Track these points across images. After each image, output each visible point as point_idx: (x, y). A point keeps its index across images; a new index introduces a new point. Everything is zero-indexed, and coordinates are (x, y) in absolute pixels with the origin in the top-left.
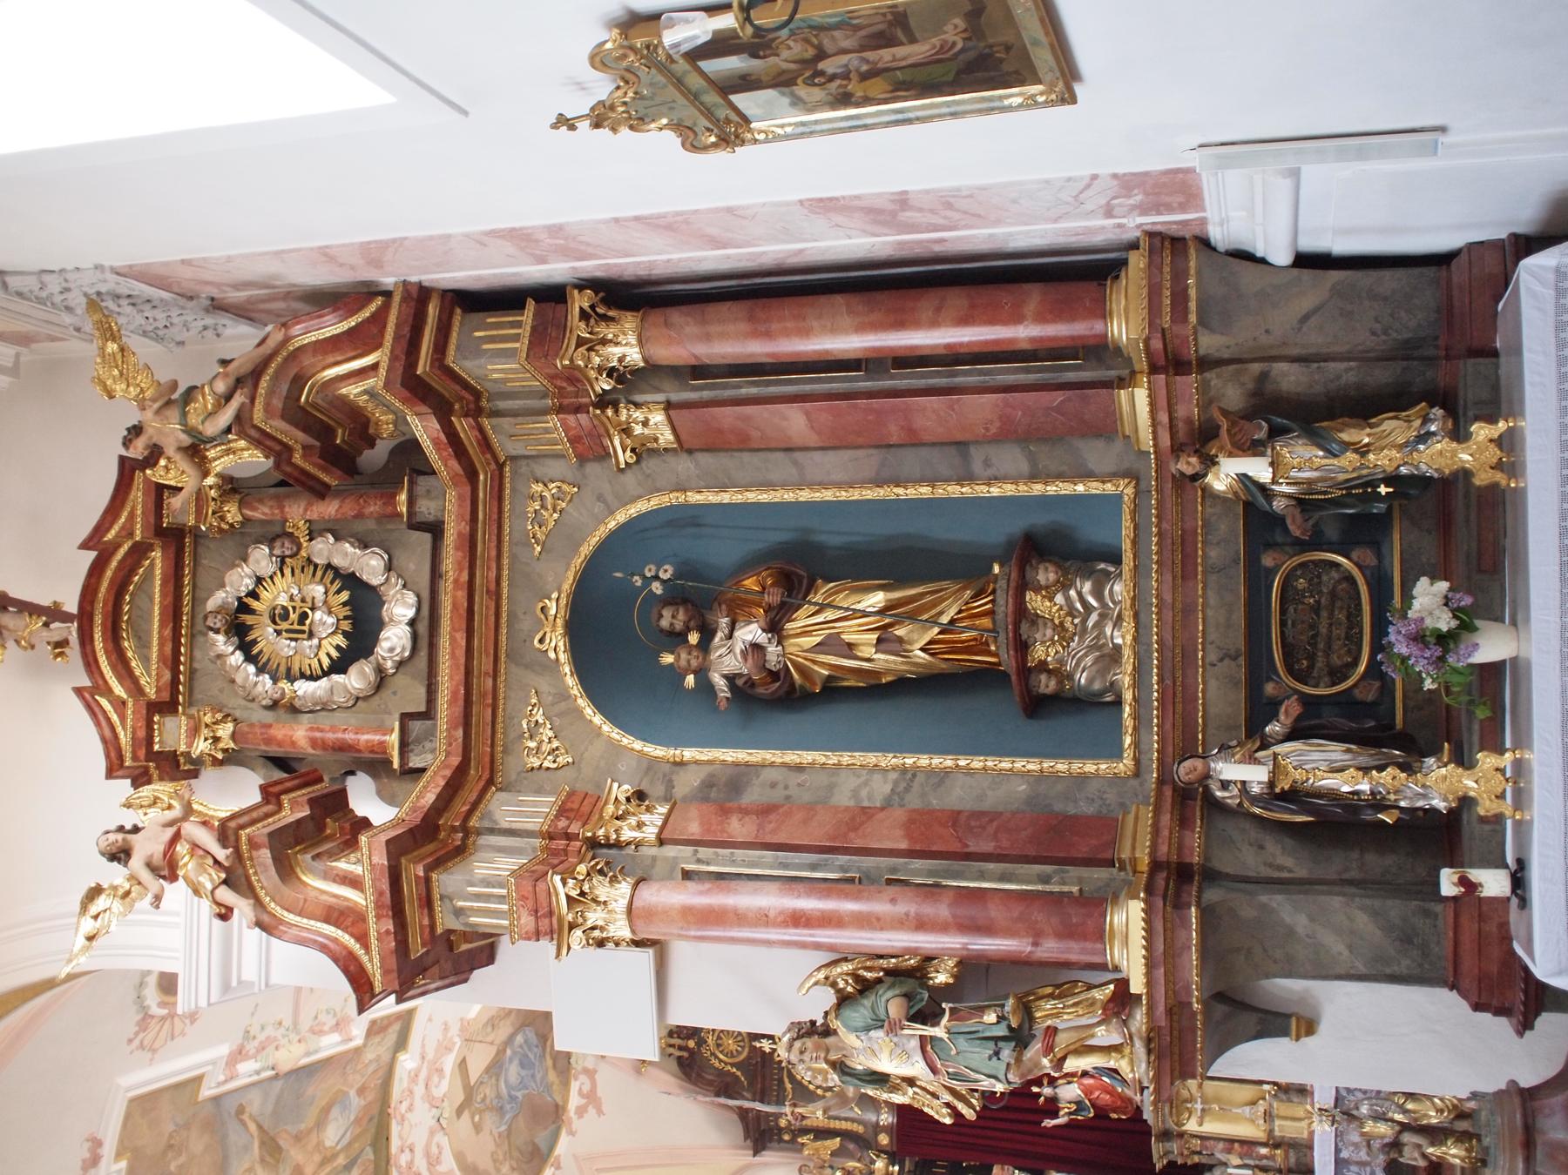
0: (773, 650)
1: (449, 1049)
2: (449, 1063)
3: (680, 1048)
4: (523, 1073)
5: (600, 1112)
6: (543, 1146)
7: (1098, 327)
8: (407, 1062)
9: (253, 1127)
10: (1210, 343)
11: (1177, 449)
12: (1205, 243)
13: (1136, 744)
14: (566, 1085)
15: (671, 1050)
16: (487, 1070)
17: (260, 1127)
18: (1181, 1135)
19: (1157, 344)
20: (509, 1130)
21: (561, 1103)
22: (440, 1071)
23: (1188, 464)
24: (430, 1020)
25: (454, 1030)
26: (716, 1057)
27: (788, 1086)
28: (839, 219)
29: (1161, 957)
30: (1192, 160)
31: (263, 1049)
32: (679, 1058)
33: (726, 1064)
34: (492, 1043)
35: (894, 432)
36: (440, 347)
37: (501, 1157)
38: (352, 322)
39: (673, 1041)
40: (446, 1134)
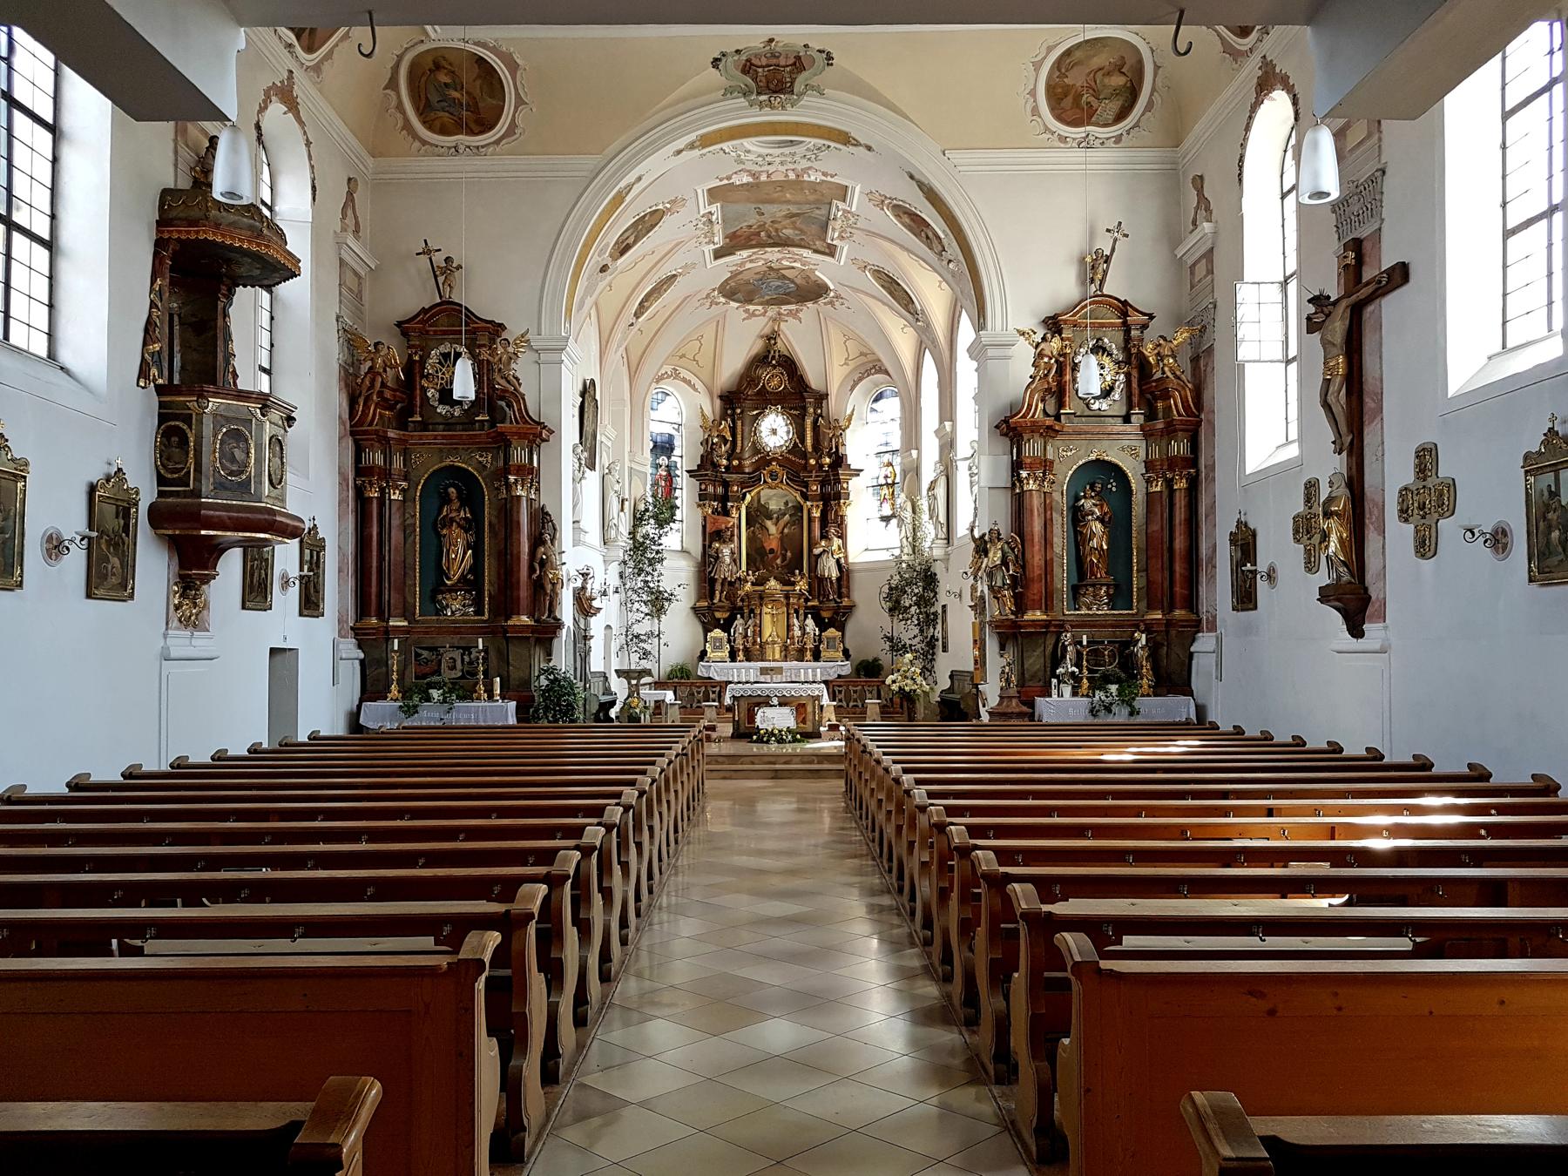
0: (1090, 517)
3: (773, 358)
6: (735, 297)
7: (1178, 605)
8: (806, 253)
10: (1173, 632)
11: (1145, 624)
12: (1198, 632)
13: (1071, 615)
14: (761, 304)
15: (772, 352)
18: (761, 605)
19: (1174, 621)
23: (1142, 627)
25: (811, 266)
26: (767, 375)
27: (755, 413)
28: (1211, 549)
29: (1034, 623)
30: (1219, 632)
32: (768, 357)
35: (1151, 553)
36: (1181, 430)
38: (1190, 400)
39: (777, 354)
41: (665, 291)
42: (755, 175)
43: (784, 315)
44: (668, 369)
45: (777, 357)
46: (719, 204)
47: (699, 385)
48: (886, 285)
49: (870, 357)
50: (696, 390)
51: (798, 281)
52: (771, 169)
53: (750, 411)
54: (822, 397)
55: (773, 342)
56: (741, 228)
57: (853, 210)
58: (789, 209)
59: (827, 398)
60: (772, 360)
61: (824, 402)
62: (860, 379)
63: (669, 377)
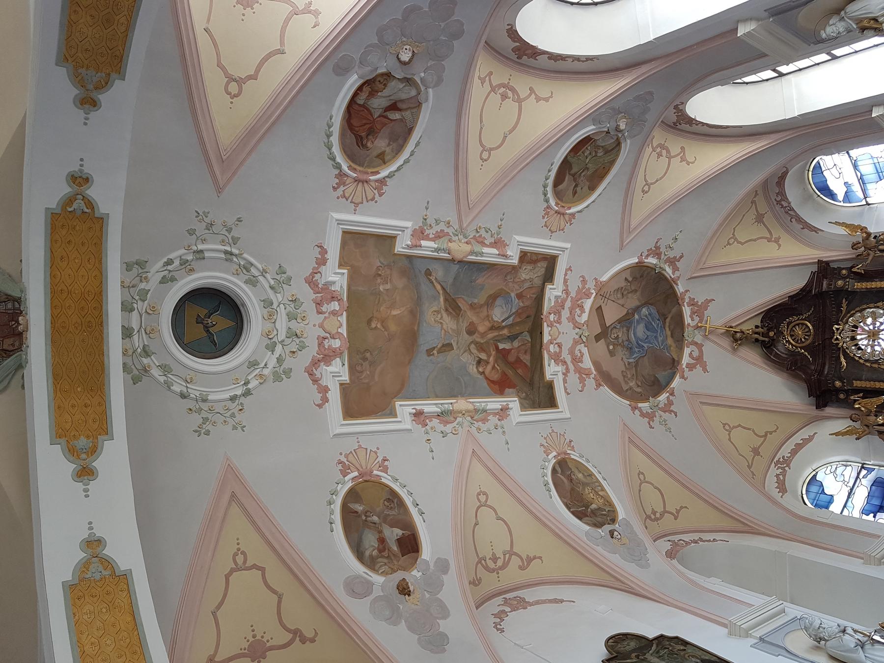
1: (588, 296)
2: (588, 304)
4: (649, 333)
5: (705, 370)
8: (553, 292)
9: (439, 287)
14: (681, 349)
15: (756, 336)
16: (620, 321)
17: (443, 288)
20: (637, 363)
21: (676, 359)
22: (581, 307)
24: (570, 269)
25: (591, 285)
27: (843, 359)
31: (440, 237)
33: (797, 347)
34: (623, 306)
37: (629, 376)
40: (585, 346)
41: (591, 475)
42: (327, 357)
43: (701, 321)
44: (774, 471)
45: (765, 330)
46: (398, 404)
47: (805, 433)
48: (584, 183)
49: (763, 207)
50: (811, 438)
51: (633, 301)
52: (312, 333)
53: (841, 368)
54: (824, 269)
55: (738, 335)
56: (483, 373)
57: (409, 224)
58: (438, 312)
59: (827, 263)
60: (769, 337)
61: (832, 265)
62: (799, 220)
63: (784, 473)
